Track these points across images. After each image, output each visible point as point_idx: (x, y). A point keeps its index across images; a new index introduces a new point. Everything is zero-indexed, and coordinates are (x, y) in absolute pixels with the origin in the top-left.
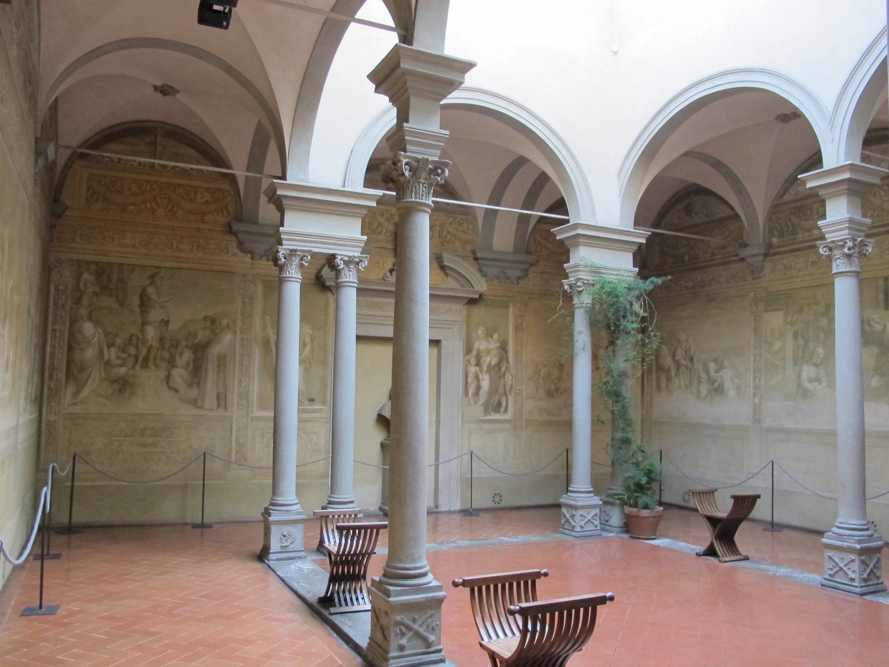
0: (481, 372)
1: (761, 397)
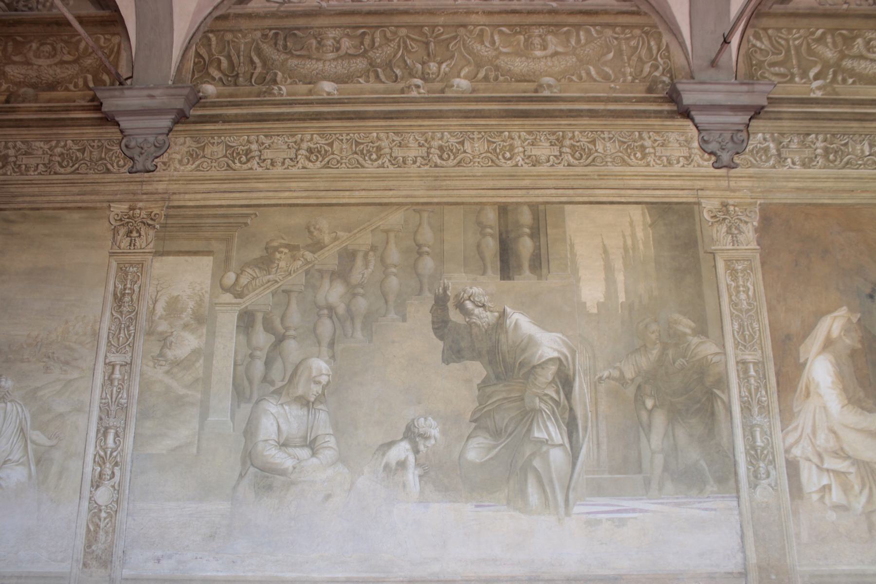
1: (117, 489)
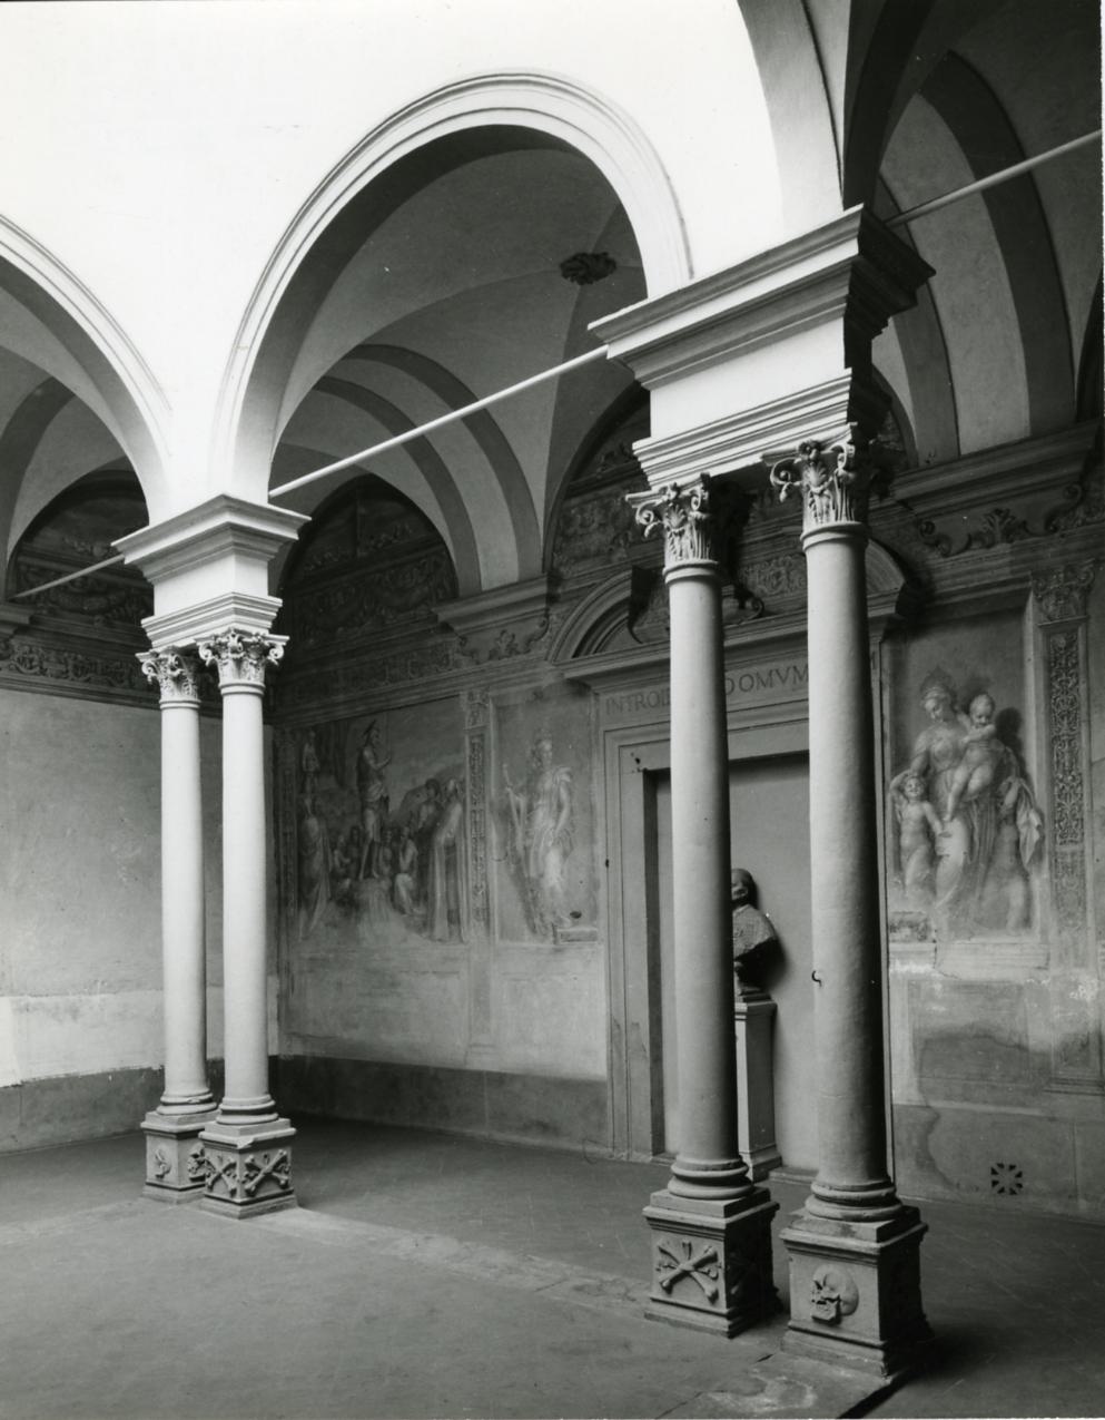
0: (939, 814)
